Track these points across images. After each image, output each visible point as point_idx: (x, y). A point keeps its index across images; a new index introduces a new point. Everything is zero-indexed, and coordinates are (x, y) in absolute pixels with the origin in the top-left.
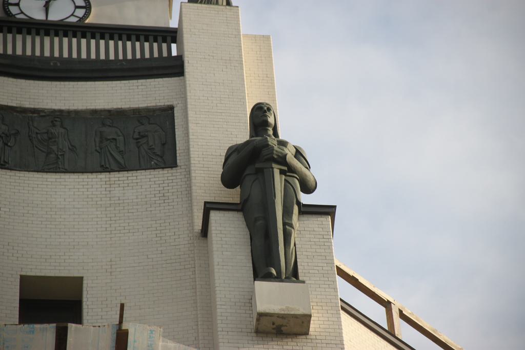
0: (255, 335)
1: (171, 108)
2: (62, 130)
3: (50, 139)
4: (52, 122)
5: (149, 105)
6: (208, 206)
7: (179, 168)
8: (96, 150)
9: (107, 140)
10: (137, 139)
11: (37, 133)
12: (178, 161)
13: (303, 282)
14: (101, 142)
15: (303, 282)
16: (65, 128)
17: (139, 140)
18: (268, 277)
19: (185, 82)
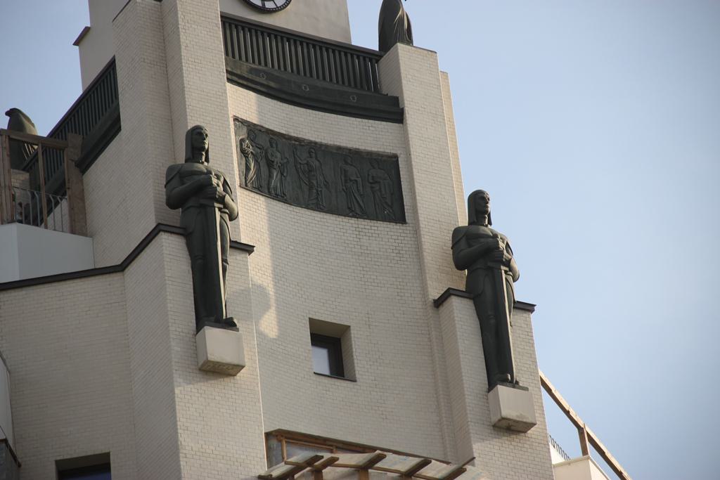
0: (492, 428)
1: (395, 157)
2: (317, 163)
3: (310, 171)
4: (309, 153)
5: (379, 150)
6: (451, 292)
7: (407, 225)
8: (343, 189)
9: (351, 180)
10: (371, 183)
11: (300, 163)
12: (406, 218)
13: (526, 389)
15: (526, 389)
16: (318, 161)
17: (373, 185)
18: (504, 381)
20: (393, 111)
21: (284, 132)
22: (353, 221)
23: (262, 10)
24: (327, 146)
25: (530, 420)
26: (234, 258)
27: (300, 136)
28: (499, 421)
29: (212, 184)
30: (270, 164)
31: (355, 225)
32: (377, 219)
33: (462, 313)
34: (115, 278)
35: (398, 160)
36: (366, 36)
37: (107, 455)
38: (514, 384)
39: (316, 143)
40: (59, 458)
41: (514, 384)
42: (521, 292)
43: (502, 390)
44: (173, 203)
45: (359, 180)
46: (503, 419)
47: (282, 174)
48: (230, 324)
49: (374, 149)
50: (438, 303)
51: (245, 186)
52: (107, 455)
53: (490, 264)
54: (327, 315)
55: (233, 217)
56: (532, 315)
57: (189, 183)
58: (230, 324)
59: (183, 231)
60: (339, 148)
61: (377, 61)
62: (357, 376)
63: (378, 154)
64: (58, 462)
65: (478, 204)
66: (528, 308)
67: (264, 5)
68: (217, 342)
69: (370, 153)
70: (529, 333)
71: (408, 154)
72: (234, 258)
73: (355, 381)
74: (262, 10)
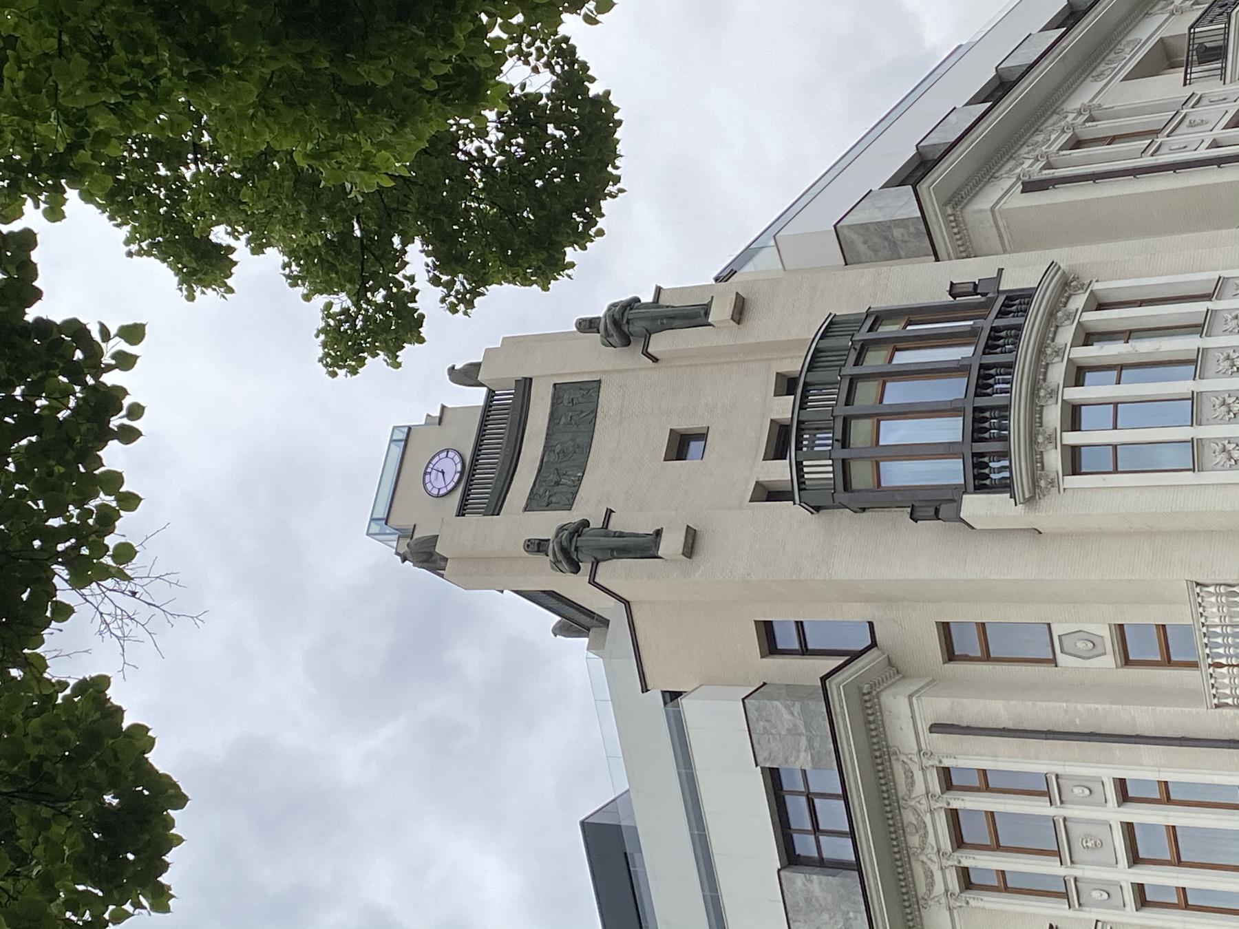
2: (558, 446)
14: (571, 424)
18: (707, 314)
19: (537, 377)
20: (525, 384)
23: (462, 473)
26: (614, 526)
28: (734, 320)
30: (557, 483)
33: (660, 343)
36: (476, 397)
42: (647, 297)
44: (576, 568)
45: (570, 414)
47: (565, 475)
48: (658, 533)
50: (655, 360)
51: (569, 506)
53: (625, 321)
55: (585, 523)
57: (560, 557)
58: (658, 533)
61: (494, 392)
64: (762, 657)
66: (659, 290)
70: (674, 290)
72: (614, 526)
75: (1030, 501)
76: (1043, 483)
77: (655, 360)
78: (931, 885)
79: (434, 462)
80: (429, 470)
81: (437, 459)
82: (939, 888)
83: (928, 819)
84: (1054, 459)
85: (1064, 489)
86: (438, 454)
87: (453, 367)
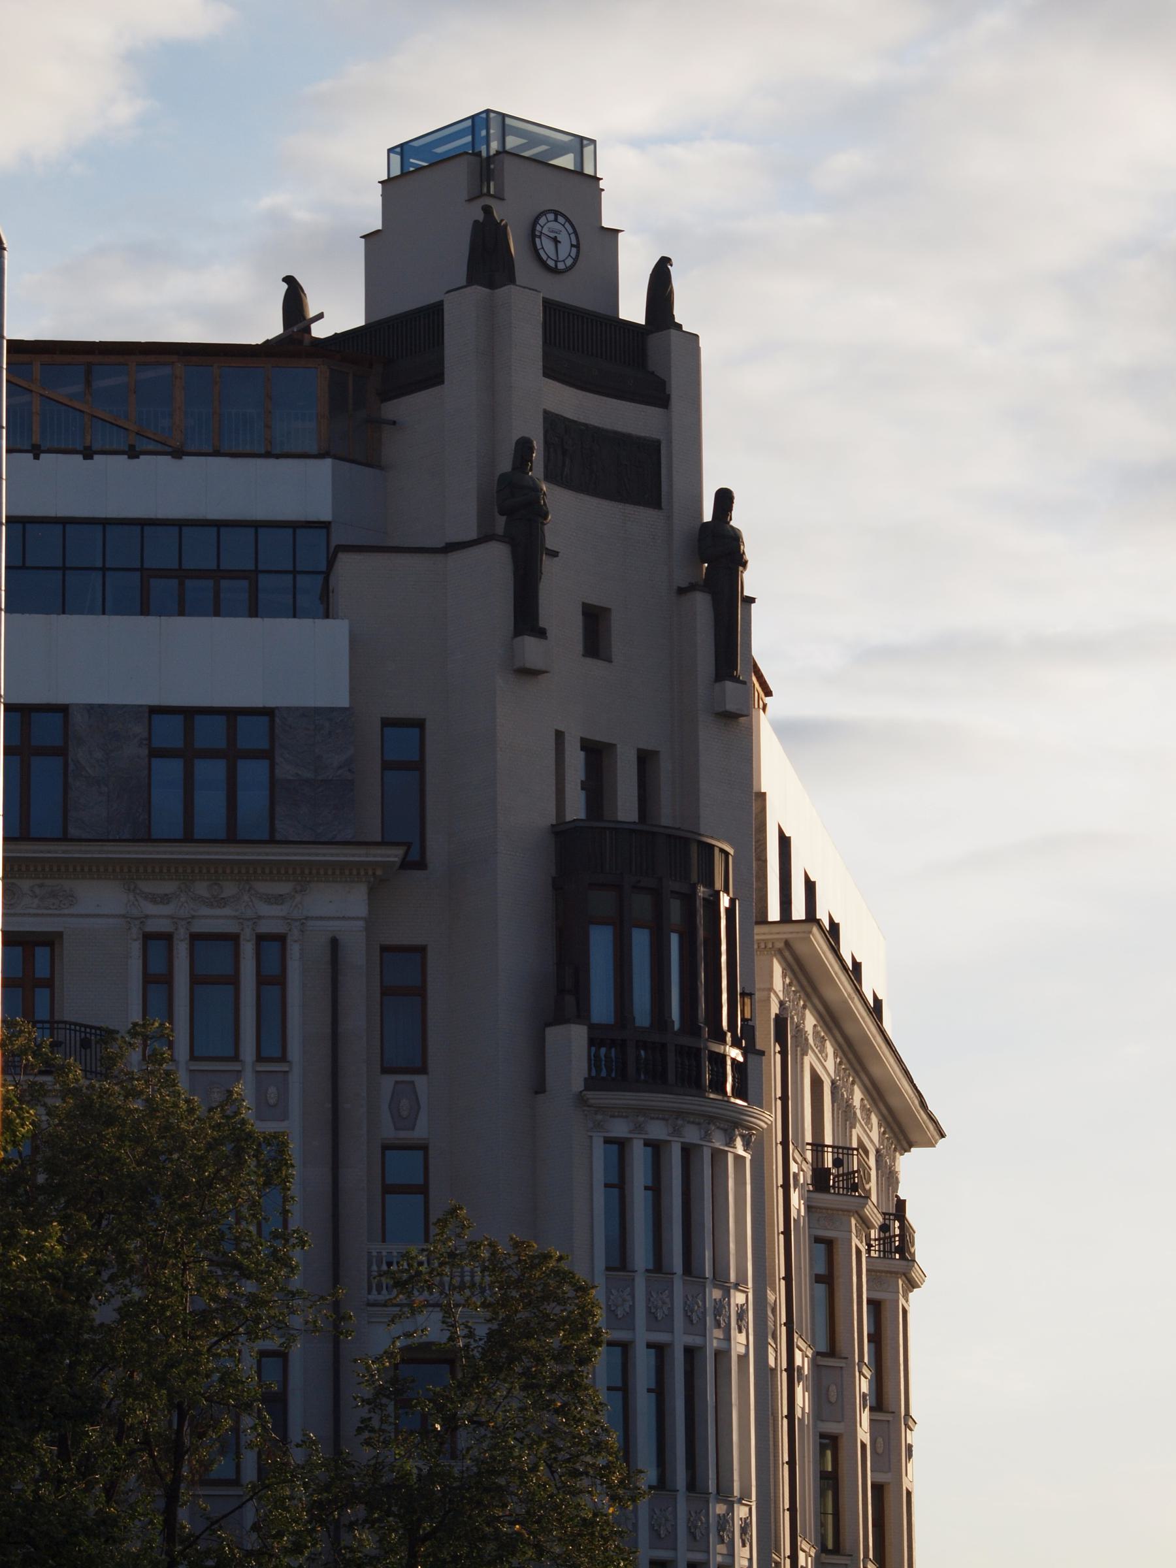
21: (575, 419)
22: (621, 506)
23: (555, 271)
24: (607, 431)
25: (745, 713)
27: (587, 422)
29: (540, 502)
31: (623, 511)
32: (638, 503)
33: (702, 603)
34: (439, 557)
35: (660, 445)
37: (424, 720)
38: (736, 680)
39: (599, 428)
40: (384, 716)
41: (736, 680)
43: (729, 685)
46: (727, 712)
49: (643, 434)
50: (681, 591)
51: (548, 478)
52: (424, 720)
54: (594, 600)
56: (753, 605)
59: (508, 538)
60: (616, 433)
62: (613, 657)
63: (644, 439)
65: (724, 499)
67: (556, 266)
68: (531, 650)
69: (639, 438)
71: (670, 441)
73: (610, 661)
74: (555, 271)
75: (581, 1100)
76: (599, 1117)
77: (681, 591)
78: (154, 899)
79: (567, 225)
80: (561, 219)
81: (571, 231)
82: (151, 909)
83: (227, 911)
84: (619, 1129)
85: (591, 1137)
86: (575, 232)
87: (671, 265)
